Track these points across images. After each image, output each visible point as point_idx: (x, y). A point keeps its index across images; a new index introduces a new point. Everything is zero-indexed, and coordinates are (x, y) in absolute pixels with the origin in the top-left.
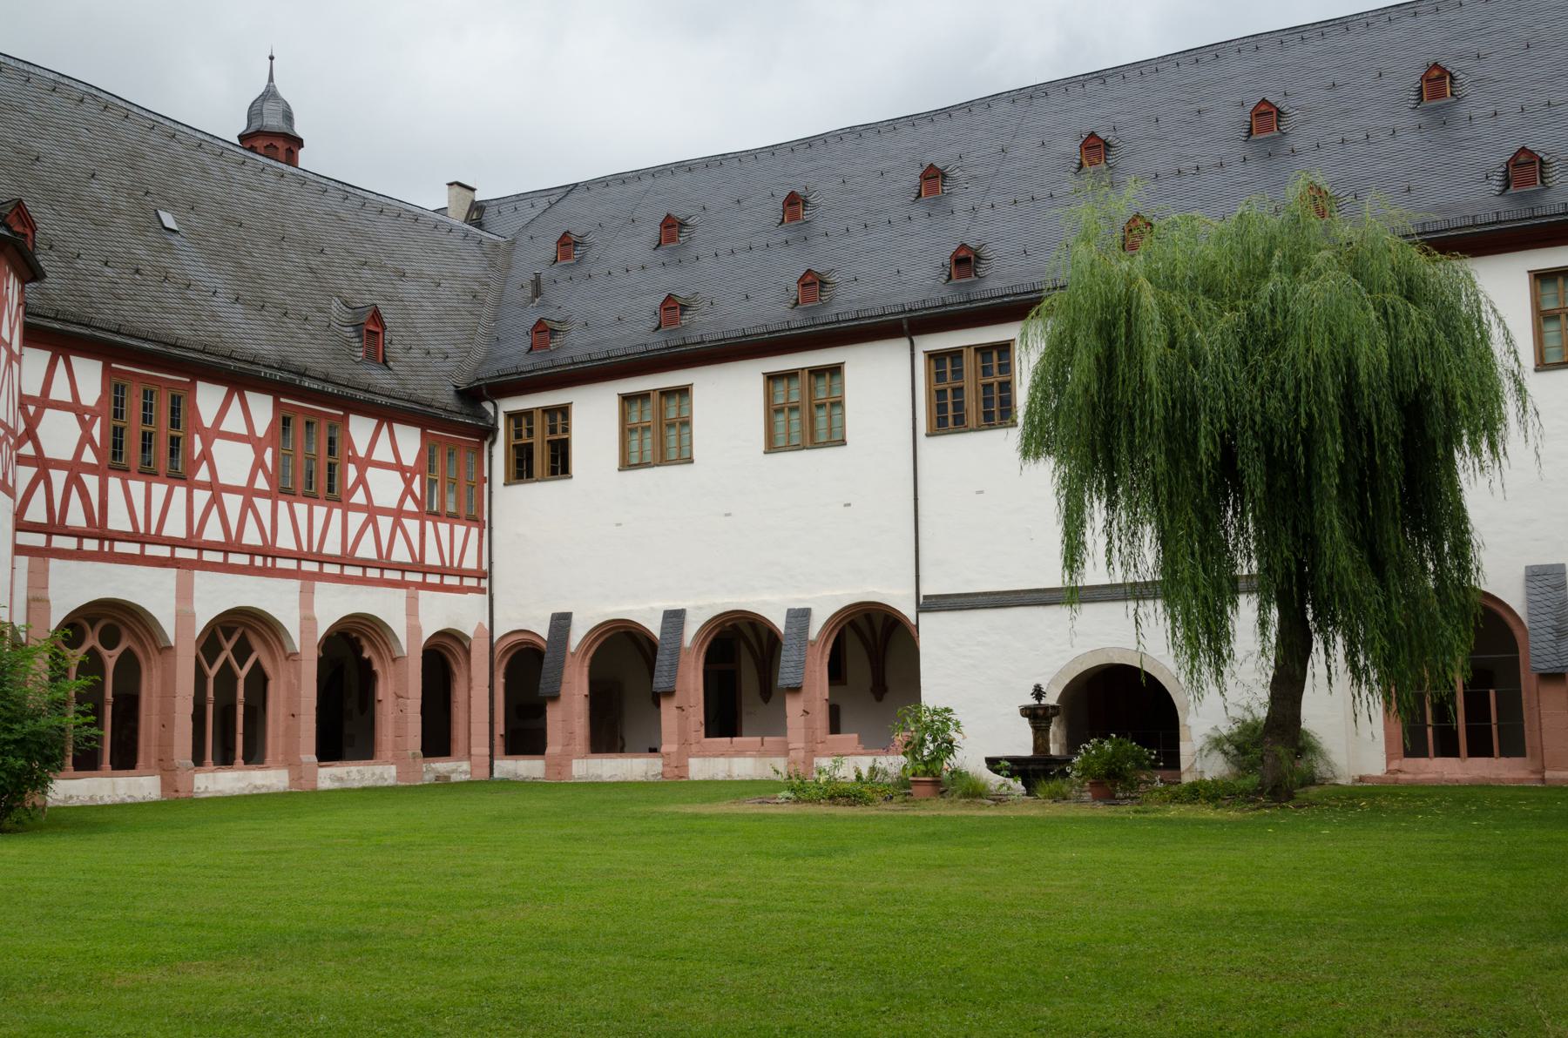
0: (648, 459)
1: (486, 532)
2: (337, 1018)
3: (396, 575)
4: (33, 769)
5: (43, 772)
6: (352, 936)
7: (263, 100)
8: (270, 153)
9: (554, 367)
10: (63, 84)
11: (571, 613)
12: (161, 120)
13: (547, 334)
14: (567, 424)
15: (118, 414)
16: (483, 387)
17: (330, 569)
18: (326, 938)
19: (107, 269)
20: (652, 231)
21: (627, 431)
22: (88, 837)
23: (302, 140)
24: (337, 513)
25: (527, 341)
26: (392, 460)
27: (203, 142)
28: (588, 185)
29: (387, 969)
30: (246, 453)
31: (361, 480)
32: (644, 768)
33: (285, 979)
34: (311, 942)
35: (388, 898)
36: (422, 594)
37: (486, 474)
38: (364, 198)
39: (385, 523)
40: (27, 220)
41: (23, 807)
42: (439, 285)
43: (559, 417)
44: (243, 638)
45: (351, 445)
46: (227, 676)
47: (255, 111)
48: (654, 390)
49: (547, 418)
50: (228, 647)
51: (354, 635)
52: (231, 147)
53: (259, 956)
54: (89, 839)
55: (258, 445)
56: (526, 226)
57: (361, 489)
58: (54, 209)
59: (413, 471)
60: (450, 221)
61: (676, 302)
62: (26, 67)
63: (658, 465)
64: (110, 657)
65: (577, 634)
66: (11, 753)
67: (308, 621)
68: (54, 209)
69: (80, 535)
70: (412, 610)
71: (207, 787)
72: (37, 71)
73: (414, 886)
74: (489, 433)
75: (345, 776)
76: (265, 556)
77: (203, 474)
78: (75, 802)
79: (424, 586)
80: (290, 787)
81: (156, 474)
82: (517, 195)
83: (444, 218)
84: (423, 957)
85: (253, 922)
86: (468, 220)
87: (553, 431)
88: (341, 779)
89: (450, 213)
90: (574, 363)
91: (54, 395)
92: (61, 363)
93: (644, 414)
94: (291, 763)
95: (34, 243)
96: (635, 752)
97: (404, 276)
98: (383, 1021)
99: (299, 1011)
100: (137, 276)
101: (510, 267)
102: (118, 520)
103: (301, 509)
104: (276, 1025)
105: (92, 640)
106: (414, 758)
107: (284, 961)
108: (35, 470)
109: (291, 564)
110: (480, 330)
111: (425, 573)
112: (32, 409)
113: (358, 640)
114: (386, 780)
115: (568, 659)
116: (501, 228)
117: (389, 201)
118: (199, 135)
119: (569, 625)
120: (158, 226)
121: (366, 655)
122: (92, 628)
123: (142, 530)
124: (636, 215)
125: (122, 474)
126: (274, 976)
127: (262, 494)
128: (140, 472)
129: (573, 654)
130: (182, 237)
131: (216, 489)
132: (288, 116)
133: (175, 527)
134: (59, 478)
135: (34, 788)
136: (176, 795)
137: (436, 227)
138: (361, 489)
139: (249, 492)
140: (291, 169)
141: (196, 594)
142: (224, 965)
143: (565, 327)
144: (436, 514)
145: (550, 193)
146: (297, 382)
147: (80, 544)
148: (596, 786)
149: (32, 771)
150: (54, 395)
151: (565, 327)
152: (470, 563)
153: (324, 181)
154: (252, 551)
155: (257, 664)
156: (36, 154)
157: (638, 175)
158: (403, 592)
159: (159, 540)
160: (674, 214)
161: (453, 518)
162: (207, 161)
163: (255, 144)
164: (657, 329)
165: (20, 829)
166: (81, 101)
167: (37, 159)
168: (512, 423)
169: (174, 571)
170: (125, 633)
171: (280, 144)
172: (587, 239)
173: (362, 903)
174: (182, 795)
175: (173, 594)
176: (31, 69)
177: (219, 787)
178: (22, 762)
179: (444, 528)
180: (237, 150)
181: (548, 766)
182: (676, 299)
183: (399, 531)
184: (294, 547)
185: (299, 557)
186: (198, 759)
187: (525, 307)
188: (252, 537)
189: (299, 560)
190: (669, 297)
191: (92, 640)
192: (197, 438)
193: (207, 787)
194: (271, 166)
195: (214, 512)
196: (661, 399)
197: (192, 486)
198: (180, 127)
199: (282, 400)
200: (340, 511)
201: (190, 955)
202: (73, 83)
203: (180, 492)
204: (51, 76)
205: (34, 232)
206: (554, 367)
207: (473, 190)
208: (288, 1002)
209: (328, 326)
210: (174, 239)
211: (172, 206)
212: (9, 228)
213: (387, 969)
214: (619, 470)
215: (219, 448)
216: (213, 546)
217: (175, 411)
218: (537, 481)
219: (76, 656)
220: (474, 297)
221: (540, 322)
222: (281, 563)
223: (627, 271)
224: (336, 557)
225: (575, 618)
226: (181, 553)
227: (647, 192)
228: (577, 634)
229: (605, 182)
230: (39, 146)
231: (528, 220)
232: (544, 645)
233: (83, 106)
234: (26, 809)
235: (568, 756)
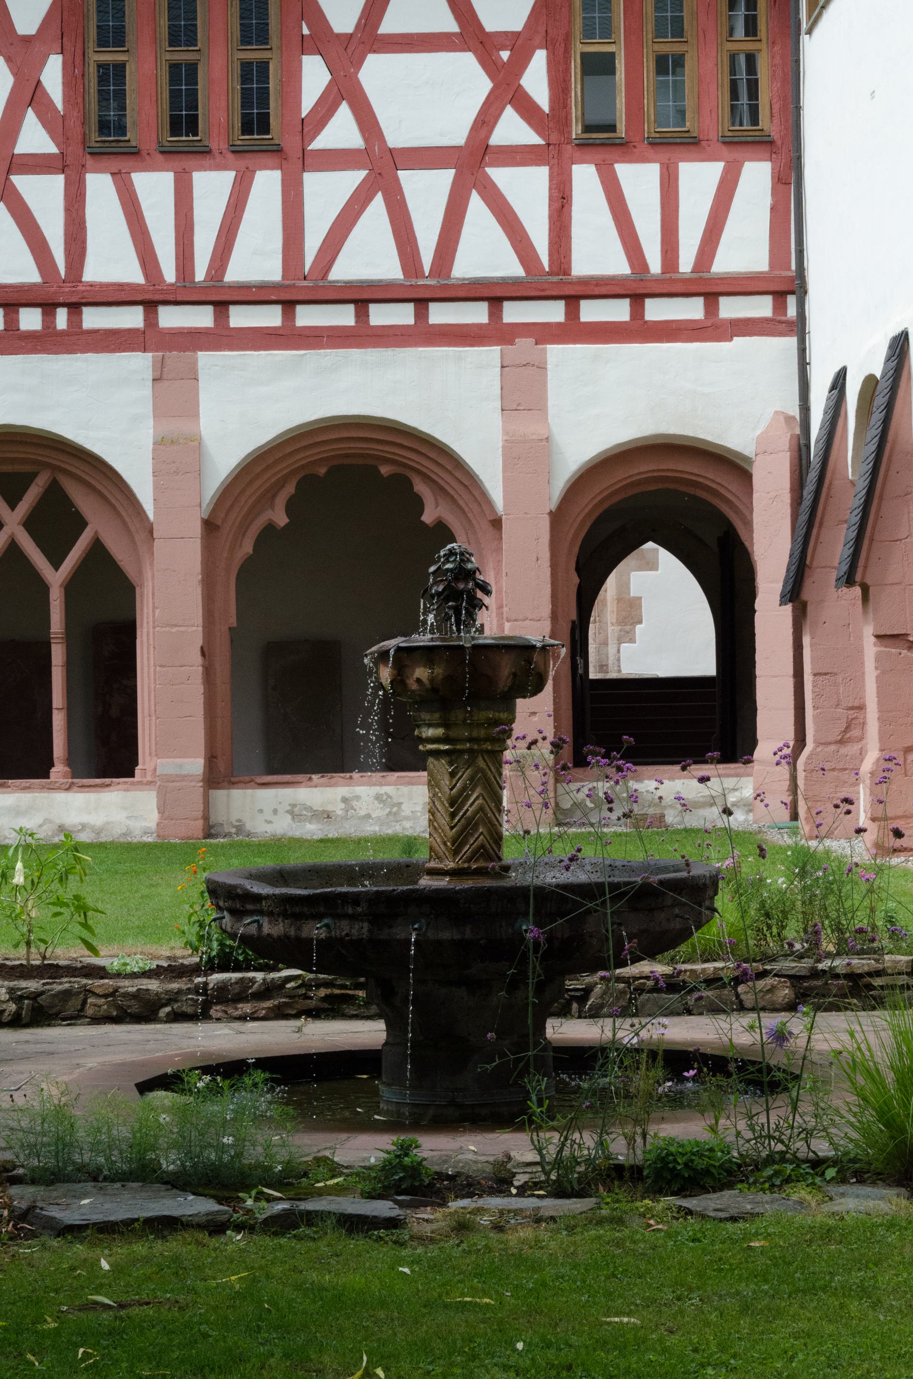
26: (452, 26)
51: (385, 470)
76: (48, 308)
121: (428, 517)
158: (491, 354)
200: (277, 175)
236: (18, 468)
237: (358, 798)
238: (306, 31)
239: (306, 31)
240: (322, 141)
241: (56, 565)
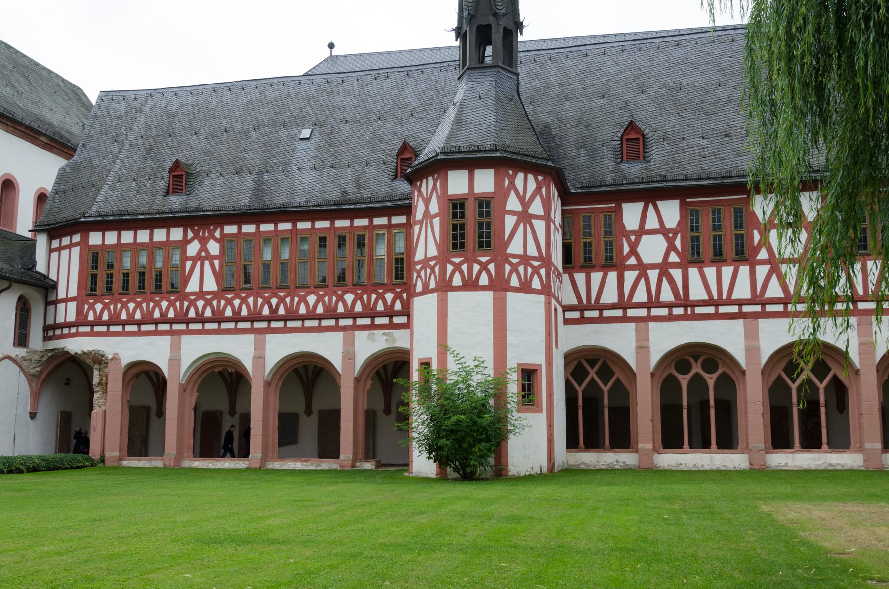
64: (711, 378)
69: (670, 306)
91: (648, 226)
92: (651, 208)
108: (637, 272)
112: (633, 238)
123: (715, 297)
125: (699, 265)
128: (712, 262)
134: (653, 275)
150: (648, 226)
169: (741, 322)
175: (743, 336)
191: (697, 368)
192: (756, 232)
226: (746, 309)
236: (593, 357)
241: (605, 386)
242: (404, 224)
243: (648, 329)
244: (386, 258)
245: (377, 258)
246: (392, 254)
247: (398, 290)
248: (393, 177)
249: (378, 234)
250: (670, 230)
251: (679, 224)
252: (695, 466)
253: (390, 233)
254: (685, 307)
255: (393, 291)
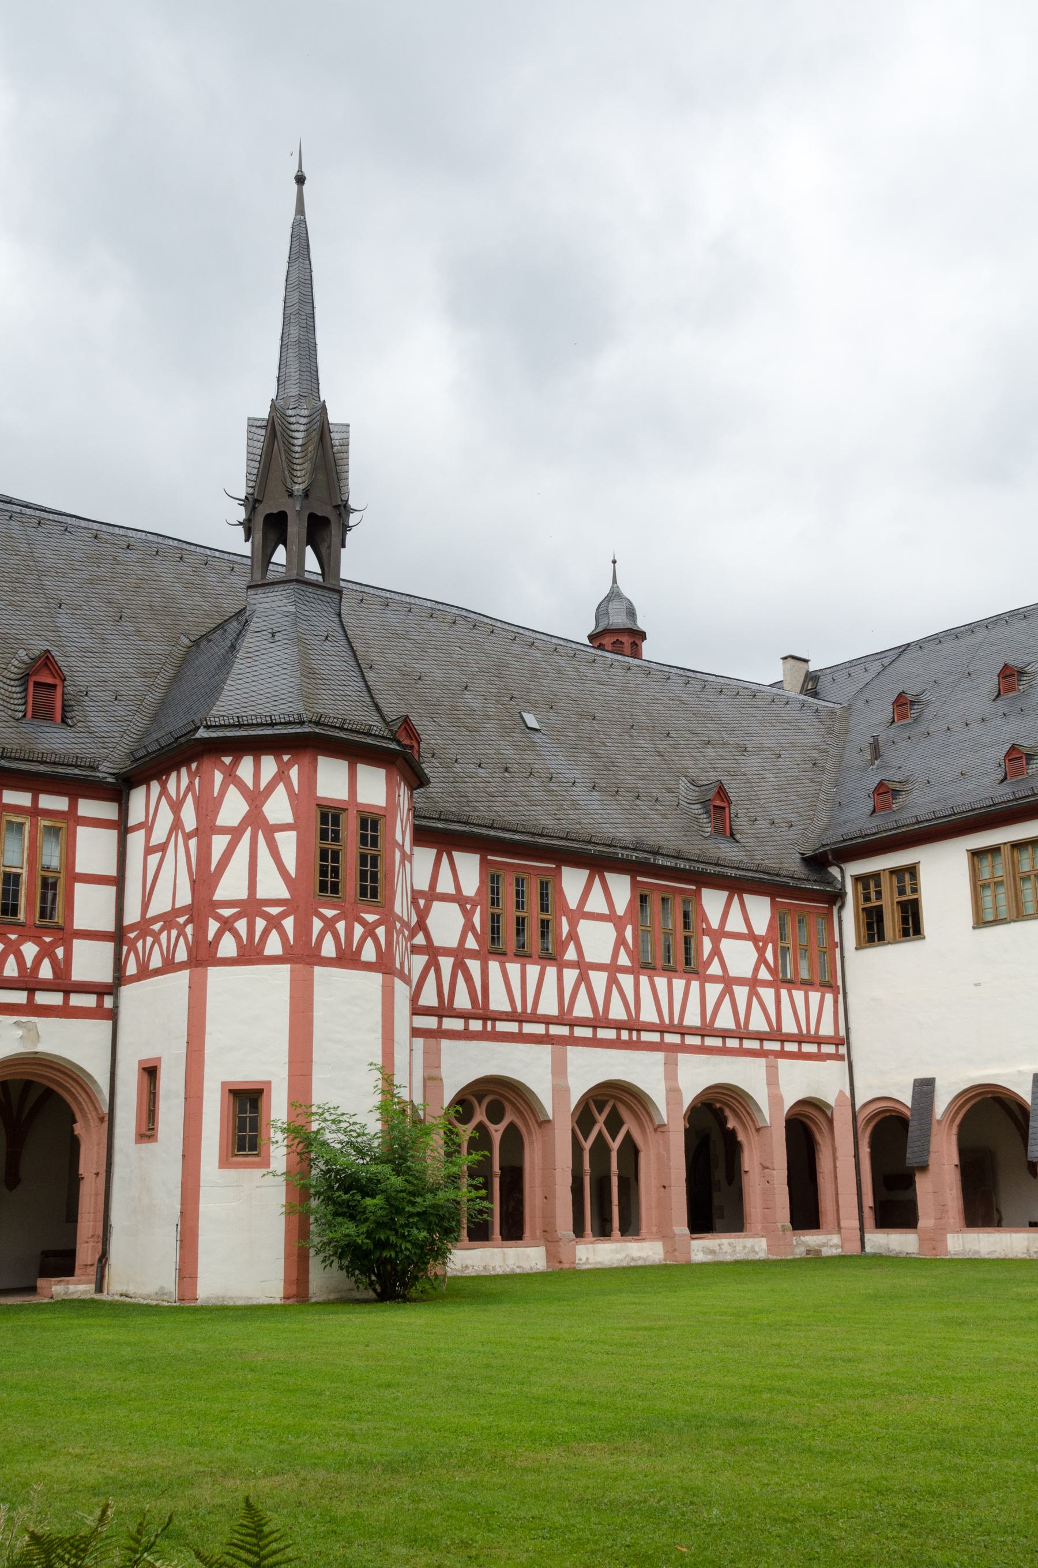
0: (1003, 913)
1: (841, 997)
2: (730, 1514)
3: (754, 1045)
4: (434, 1240)
5: (443, 1243)
6: (737, 1423)
7: (609, 601)
8: (617, 648)
9: (898, 828)
10: (438, 610)
11: (934, 1079)
12: (521, 631)
13: (888, 796)
14: (916, 884)
15: (495, 902)
16: (829, 853)
17: (692, 1040)
18: (712, 1424)
19: (480, 770)
20: (990, 682)
21: (978, 887)
22: (484, 1307)
23: (644, 633)
24: (695, 985)
25: (870, 804)
26: (745, 931)
27: (558, 646)
28: (920, 645)
29: (775, 1462)
30: (608, 931)
31: (716, 952)
32: (1026, 1243)
33: (675, 1466)
34: (697, 1428)
35: (769, 1382)
36: (782, 1062)
37: (837, 939)
38: (704, 681)
39: (741, 993)
40: (413, 733)
41: (427, 1277)
42: (779, 756)
43: (907, 877)
44: (614, 1112)
45: (704, 918)
46: (601, 1149)
47: (601, 612)
48: (1005, 844)
49: (895, 879)
50: (601, 1119)
51: (718, 1105)
52: (583, 648)
53: (649, 1440)
54: (485, 1310)
55: (619, 924)
56: (861, 691)
57: (716, 961)
58: (435, 721)
59: (765, 940)
60: (786, 693)
61: (1020, 752)
62: (408, 599)
63: (1014, 921)
64: (496, 1131)
65: (942, 1103)
66: (415, 1225)
67: (673, 1092)
68: (435, 721)
70: (773, 1080)
71: (587, 1259)
72: (417, 601)
73: (795, 1370)
74: (837, 898)
75: (717, 1249)
76: (630, 1030)
77: (571, 954)
78: (470, 1272)
79: (784, 1054)
80: (665, 1260)
81: (529, 956)
82: (850, 662)
83: (780, 692)
84: (810, 1450)
85: (640, 1403)
86: (804, 691)
87: (902, 891)
88: (713, 1252)
89: (786, 685)
90: (918, 822)
93: (994, 869)
94: (664, 1235)
95: (419, 752)
96: (1013, 1226)
97: (745, 751)
98: (775, 1520)
99: (692, 1503)
100: (507, 775)
101: (847, 732)
102: (498, 1002)
103: (661, 982)
104: (670, 1517)
105: (480, 1116)
106: (783, 1231)
107: (672, 1447)
109: (655, 1037)
110: (822, 796)
111: (782, 1042)
113: (721, 1110)
114: (757, 1253)
115: (935, 1127)
116: (836, 695)
117: (728, 681)
118: (554, 640)
119: (933, 1091)
120: (523, 727)
121: (730, 1125)
122: (480, 1103)
124: (972, 668)
126: (665, 1462)
127: (624, 970)
129: (939, 1122)
130: (544, 734)
131: (583, 967)
132: (631, 613)
133: (548, 1006)
135: (435, 1260)
136: (561, 1266)
137: (773, 701)
138: (716, 961)
139: (612, 969)
140: (636, 662)
141: (569, 1069)
142: (616, 1448)
143: (907, 787)
144: (790, 982)
145: (883, 655)
146: (652, 860)
147: (467, 1024)
148: (975, 1263)
149: (433, 1243)
151: (907, 787)
152: (827, 1029)
153: (667, 669)
154: (618, 1026)
155: (628, 1136)
156: (418, 674)
157: (971, 628)
158: (762, 1061)
159: (535, 1018)
160: (1011, 663)
161: (807, 985)
162: (563, 663)
163: (604, 642)
164: (1002, 781)
165: (424, 1298)
166: (454, 623)
167: (420, 679)
168: (860, 887)
170: (508, 1107)
171: (626, 640)
172: (923, 698)
173: (744, 1387)
174: (566, 1266)
176: (412, 600)
177: (599, 1259)
178: (424, 1234)
179: (799, 995)
180: (588, 649)
181: (921, 1240)
182: (1021, 748)
183: (755, 1000)
184: (657, 1021)
185: (662, 1029)
186: (579, 1230)
187: (864, 770)
188: (617, 1012)
189: (662, 1032)
190: (1013, 748)
191: (480, 1116)
192: (564, 919)
193: (587, 1259)
194: (618, 661)
195: (583, 991)
196: (1012, 852)
197: (562, 966)
198: (538, 636)
199: (639, 879)
201: (584, 1436)
202: (447, 608)
203: (551, 971)
204: (429, 604)
205: (419, 743)
206: (898, 828)
207: (806, 661)
208: (680, 1492)
209: (677, 806)
210: (537, 737)
211: (534, 707)
212: (399, 743)
213: (775, 1462)
214: (974, 928)
215: (585, 927)
216: (583, 1023)
217: (544, 896)
218: (889, 943)
219: (466, 1132)
220: (814, 764)
221: (881, 784)
222: (646, 1036)
223: (967, 725)
224: (697, 1028)
225: (938, 1083)
226: (555, 1030)
227: (981, 644)
228: (942, 1103)
229: (937, 639)
230: (420, 667)
231: (862, 684)
232: (908, 1113)
233: (455, 627)
234: (430, 1279)
235: (941, 1231)
237: (723, 1244)
238: (704, 927)
239: (704, 927)
240: (710, 972)
242: (63, 812)
243: (440, 1050)
244: (24, 872)
245: (8, 869)
246: (38, 867)
247: (48, 939)
248: (21, 714)
249: (9, 822)
250: (468, 900)
251: (479, 891)
252: (485, 1268)
253: (34, 826)
254: (485, 1019)
255: (37, 940)
